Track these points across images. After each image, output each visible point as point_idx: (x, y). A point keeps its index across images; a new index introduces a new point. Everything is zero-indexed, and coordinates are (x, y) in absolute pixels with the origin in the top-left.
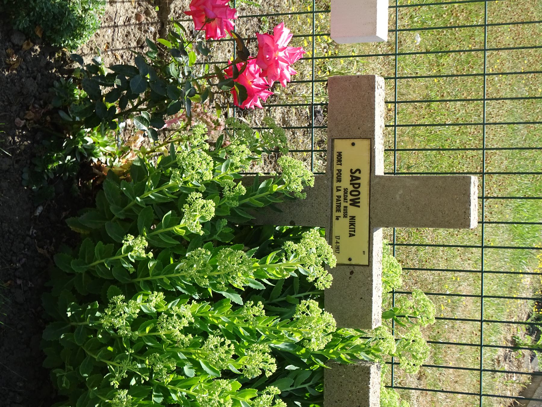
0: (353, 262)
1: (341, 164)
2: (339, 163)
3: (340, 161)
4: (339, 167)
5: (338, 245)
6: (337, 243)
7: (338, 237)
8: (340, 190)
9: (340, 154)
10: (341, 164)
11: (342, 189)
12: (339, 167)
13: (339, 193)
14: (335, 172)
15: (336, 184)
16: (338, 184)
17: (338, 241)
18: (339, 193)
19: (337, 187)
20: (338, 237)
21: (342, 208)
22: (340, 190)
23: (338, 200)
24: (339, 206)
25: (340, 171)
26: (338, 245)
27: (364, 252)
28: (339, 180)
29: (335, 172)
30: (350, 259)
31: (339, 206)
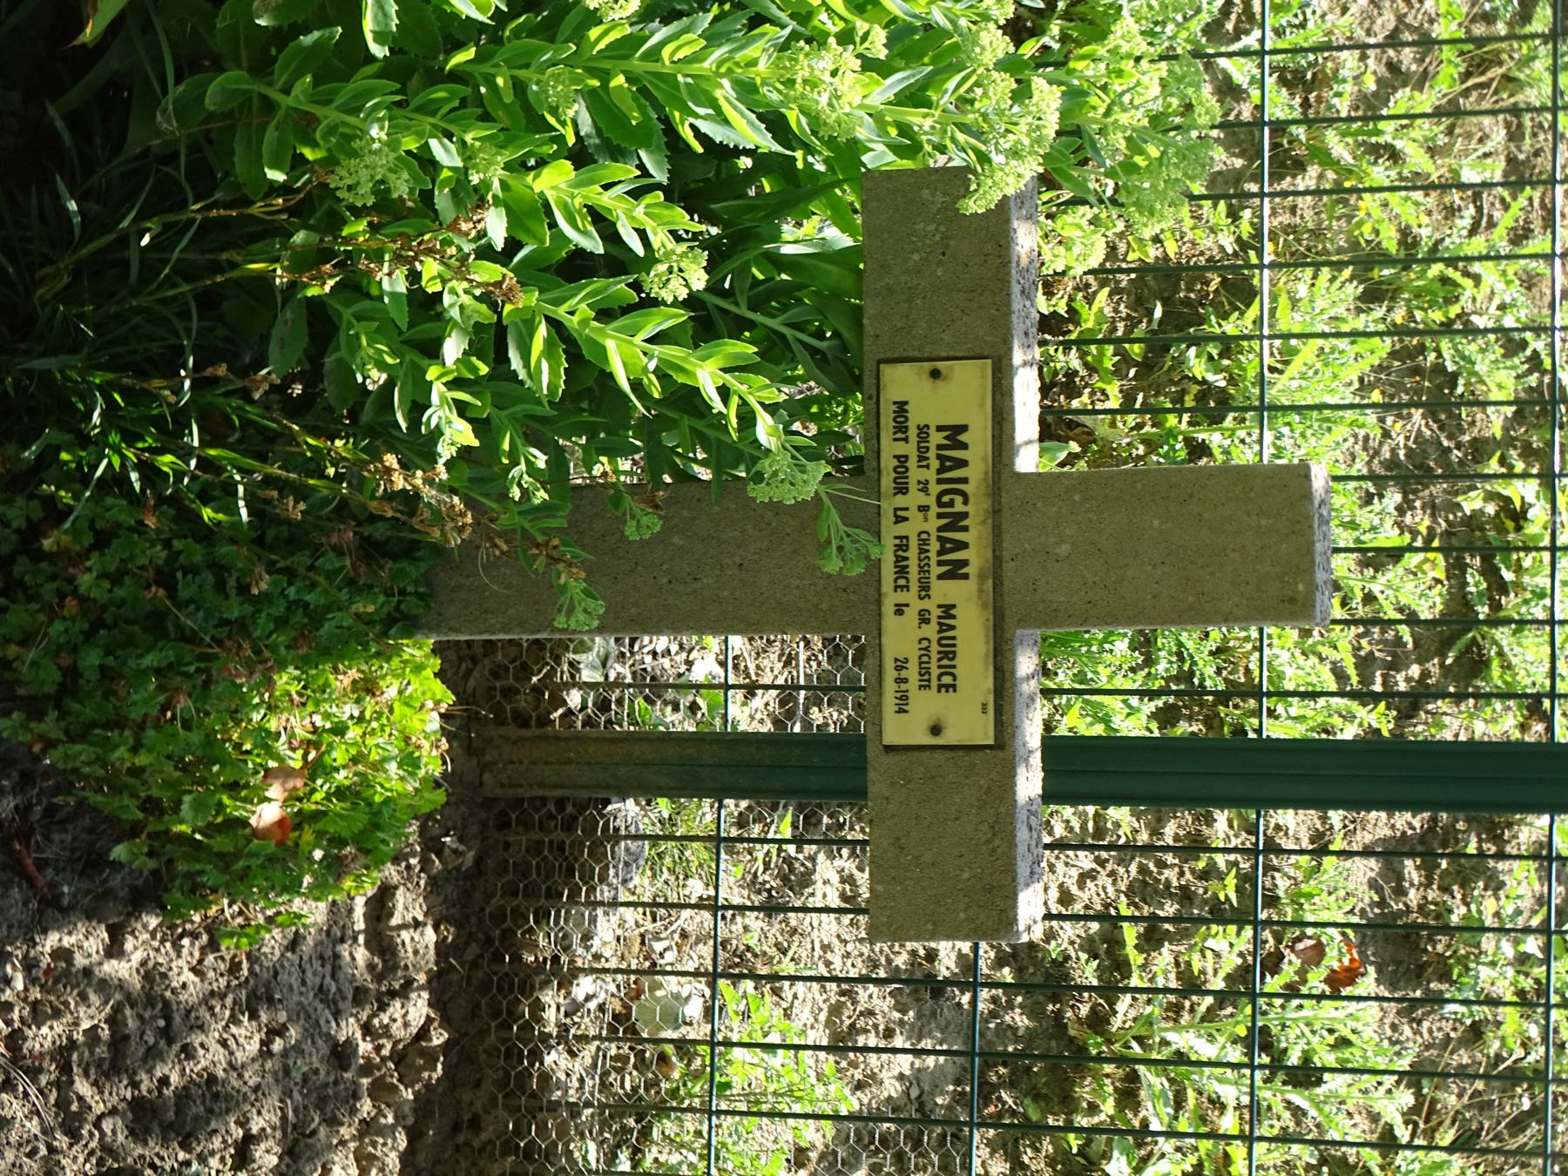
0: (949, 737)
1: (906, 440)
3: (901, 428)
4: (901, 449)
5: (904, 687)
9: (901, 407)
10: (906, 440)
14: (888, 463)
17: (904, 674)
18: (902, 529)
23: (900, 547)
24: (902, 571)
27: (984, 706)
29: (888, 463)
31: (902, 571)
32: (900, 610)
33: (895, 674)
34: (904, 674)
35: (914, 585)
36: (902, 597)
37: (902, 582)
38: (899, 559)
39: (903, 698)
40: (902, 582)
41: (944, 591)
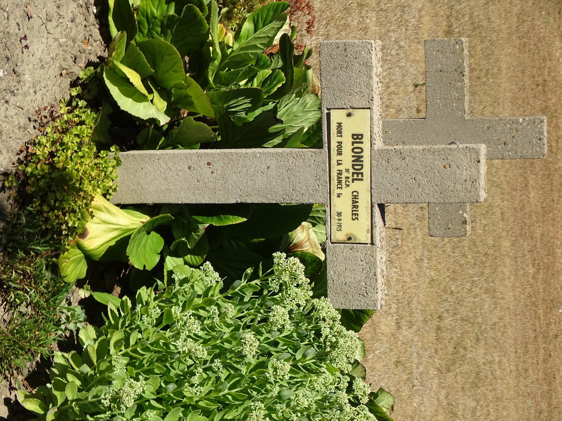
1: (341, 136)
2: (339, 135)
3: (340, 132)
4: (339, 139)
5: (340, 222)
6: (340, 220)
7: (339, 214)
8: (341, 164)
9: (340, 125)
10: (341, 136)
12: (339, 139)
13: (340, 167)
15: (335, 157)
16: (339, 158)
17: (340, 218)
18: (340, 167)
19: (338, 161)
20: (339, 214)
21: (343, 184)
22: (341, 164)
24: (340, 182)
25: (340, 143)
26: (340, 222)
28: (340, 153)
31: (340, 182)
32: (339, 196)
33: (337, 217)
34: (340, 218)
35: (344, 186)
36: (339, 191)
37: (340, 186)
38: (339, 178)
39: (340, 226)
40: (340, 186)
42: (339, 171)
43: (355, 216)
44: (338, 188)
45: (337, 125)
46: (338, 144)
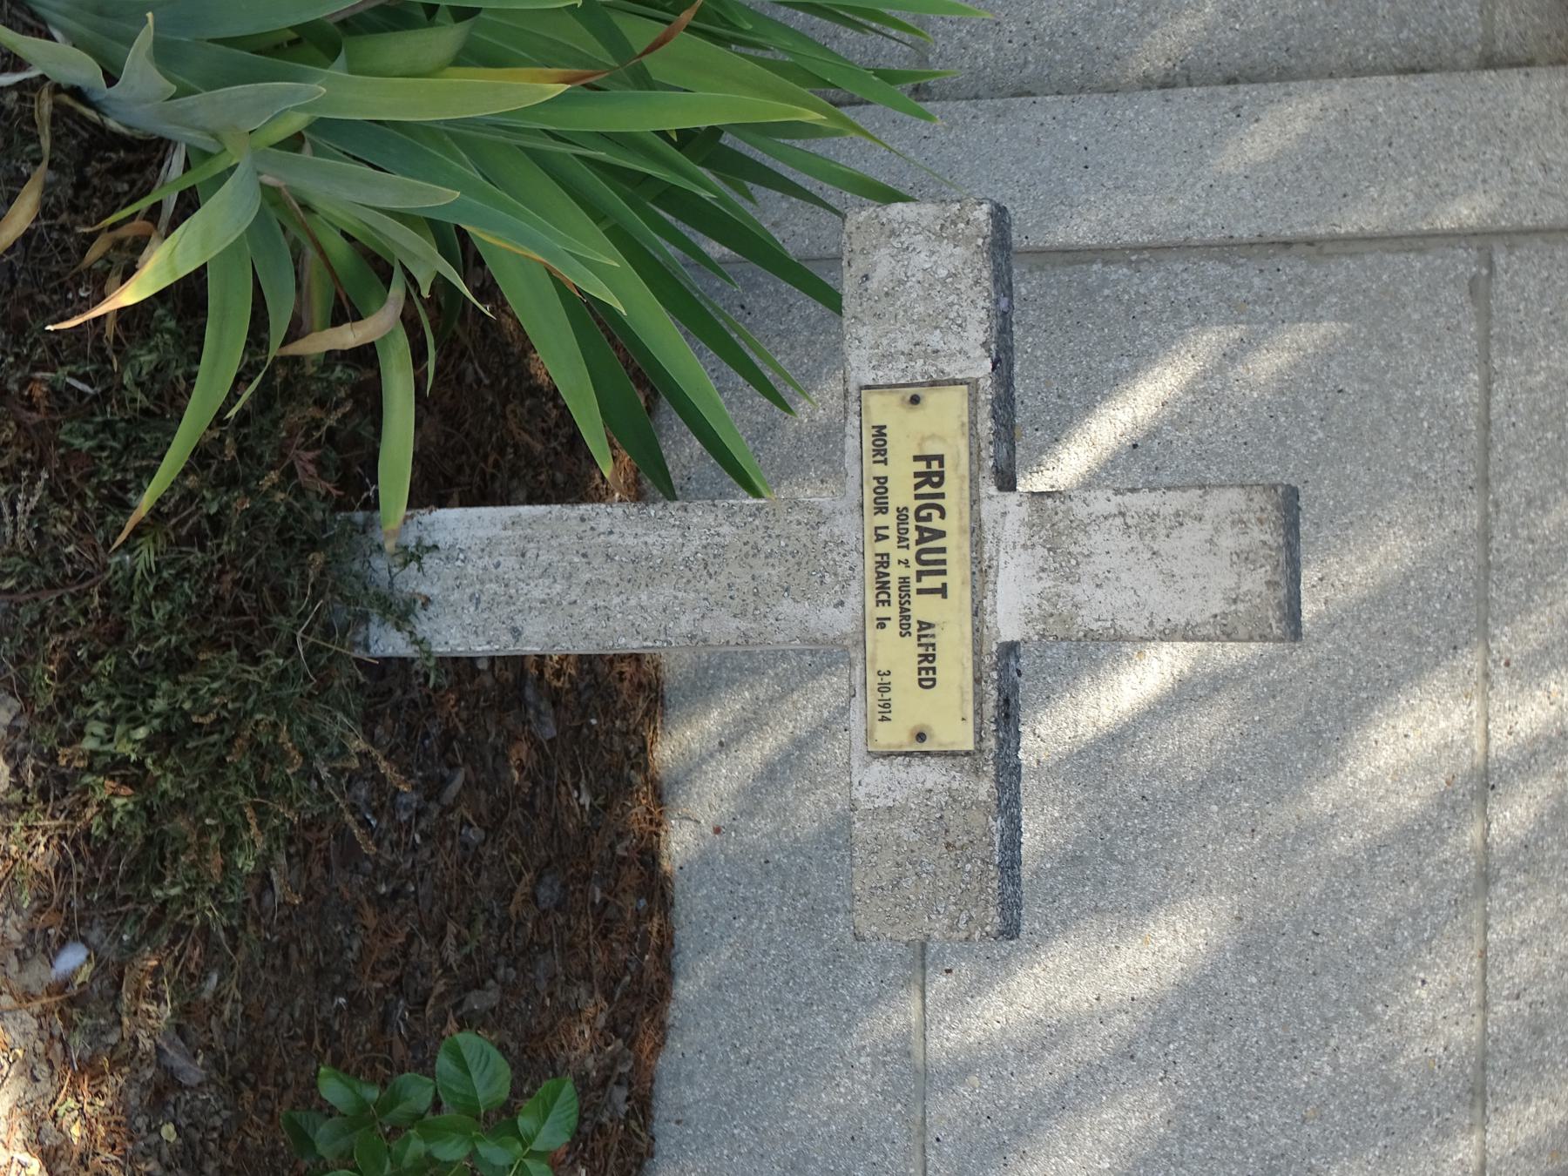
1: (885, 462)
2: (879, 458)
3: (880, 451)
4: (880, 470)
5: (886, 696)
9: (880, 431)
10: (885, 462)
11: (893, 533)
12: (880, 470)
13: (882, 547)
14: (870, 485)
16: (880, 520)
18: (882, 547)
19: (877, 528)
23: (881, 564)
25: (882, 481)
26: (886, 696)
28: (882, 509)
30: (921, 737)
31: (883, 587)
35: (895, 599)
36: (883, 611)
37: (883, 597)
38: (880, 575)
39: (886, 705)
40: (883, 597)
41: (922, 608)
42: (882, 555)
43: (927, 679)
44: (878, 602)
45: (874, 432)
46: (875, 484)
